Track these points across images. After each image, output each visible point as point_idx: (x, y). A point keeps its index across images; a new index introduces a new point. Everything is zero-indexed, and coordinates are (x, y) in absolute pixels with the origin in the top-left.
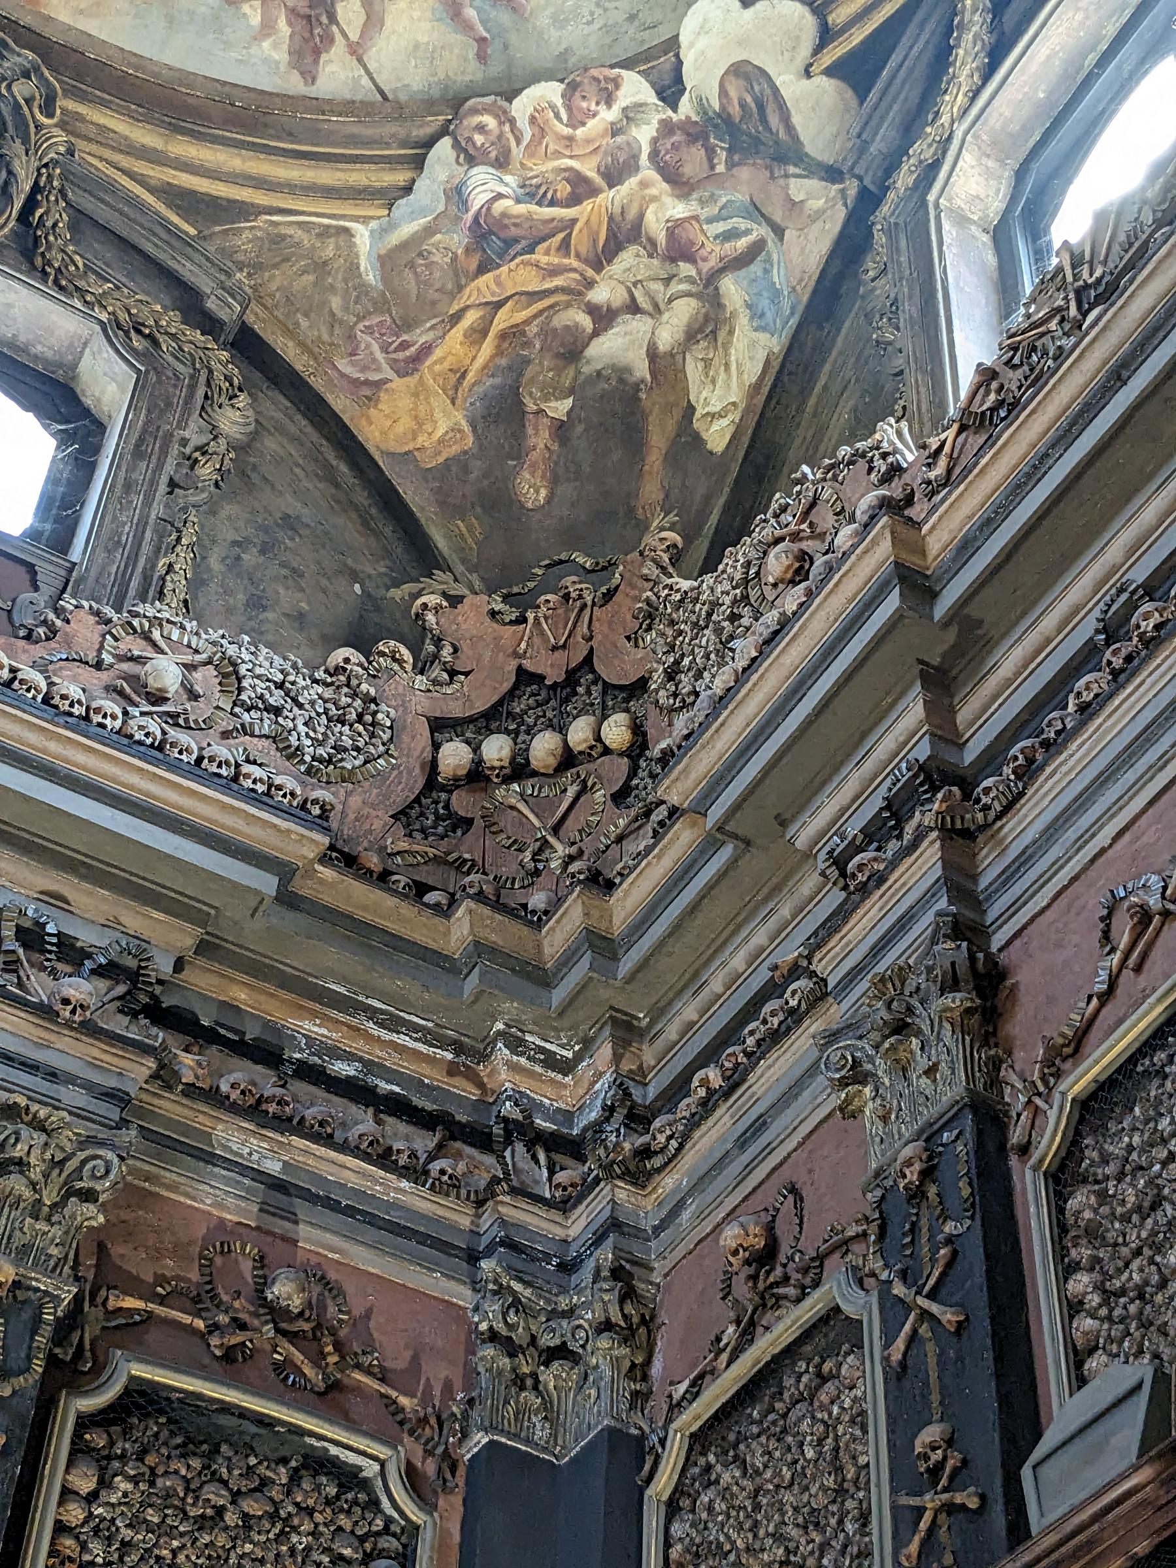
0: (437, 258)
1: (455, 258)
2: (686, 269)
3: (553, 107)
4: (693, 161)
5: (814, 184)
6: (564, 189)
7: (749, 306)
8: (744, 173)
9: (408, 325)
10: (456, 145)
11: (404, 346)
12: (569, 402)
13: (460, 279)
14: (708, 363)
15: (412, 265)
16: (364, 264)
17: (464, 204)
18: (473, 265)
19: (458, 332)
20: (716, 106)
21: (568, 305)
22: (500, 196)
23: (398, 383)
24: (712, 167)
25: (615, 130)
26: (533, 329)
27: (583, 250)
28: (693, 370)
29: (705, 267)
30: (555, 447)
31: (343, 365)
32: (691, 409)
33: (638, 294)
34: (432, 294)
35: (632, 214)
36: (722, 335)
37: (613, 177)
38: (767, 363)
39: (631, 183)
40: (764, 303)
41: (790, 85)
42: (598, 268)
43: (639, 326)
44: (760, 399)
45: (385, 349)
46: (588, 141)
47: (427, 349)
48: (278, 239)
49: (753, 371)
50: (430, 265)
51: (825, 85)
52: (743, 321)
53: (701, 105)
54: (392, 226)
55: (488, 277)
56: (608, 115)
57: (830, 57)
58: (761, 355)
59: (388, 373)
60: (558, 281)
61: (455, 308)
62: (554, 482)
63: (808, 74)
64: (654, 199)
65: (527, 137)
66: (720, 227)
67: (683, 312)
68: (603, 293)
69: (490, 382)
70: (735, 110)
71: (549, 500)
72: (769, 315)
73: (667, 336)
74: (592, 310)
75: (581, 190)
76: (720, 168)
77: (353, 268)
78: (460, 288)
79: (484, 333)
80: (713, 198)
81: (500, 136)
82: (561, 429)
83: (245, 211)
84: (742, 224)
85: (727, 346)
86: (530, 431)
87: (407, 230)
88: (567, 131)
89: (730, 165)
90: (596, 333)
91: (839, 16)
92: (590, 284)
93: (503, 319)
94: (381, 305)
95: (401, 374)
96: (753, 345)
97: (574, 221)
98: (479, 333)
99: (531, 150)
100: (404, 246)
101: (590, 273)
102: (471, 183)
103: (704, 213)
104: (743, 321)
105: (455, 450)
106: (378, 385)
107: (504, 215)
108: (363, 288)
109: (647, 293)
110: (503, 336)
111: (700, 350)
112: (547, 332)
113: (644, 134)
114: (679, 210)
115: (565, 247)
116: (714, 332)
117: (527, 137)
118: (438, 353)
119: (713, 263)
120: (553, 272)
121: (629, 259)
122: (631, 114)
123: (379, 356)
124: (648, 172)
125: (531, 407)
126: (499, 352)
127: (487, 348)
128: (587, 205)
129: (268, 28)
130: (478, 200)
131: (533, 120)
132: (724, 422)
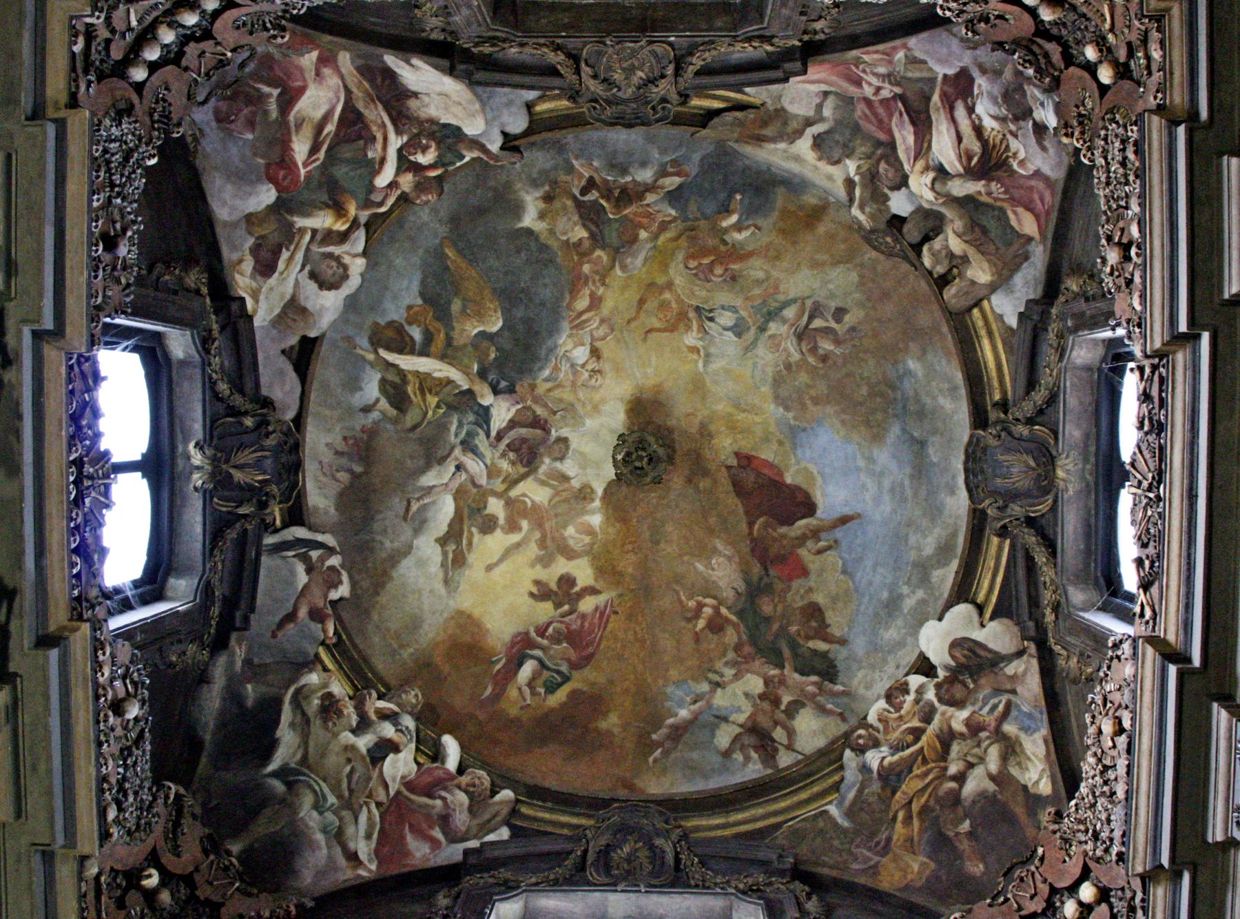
0: (871, 799)
1: (879, 795)
2: (983, 735)
3: (885, 710)
4: (958, 691)
5: (1015, 663)
6: (910, 738)
7: (1021, 729)
8: (983, 681)
9: (873, 834)
10: (853, 750)
11: (878, 843)
12: (967, 822)
13: (886, 800)
14: (1019, 764)
15: (862, 809)
16: (839, 820)
17: (870, 770)
18: (889, 792)
19: (899, 825)
20: (953, 664)
21: (941, 784)
22: (883, 758)
23: (884, 860)
24: (967, 688)
25: (917, 701)
26: (932, 802)
27: (933, 756)
28: (1014, 771)
29: (992, 728)
30: (974, 843)
31: (855, 866)
32: (1025, 787)
33: (970, 759)
34: (878, 815)
35: (945, 728)
36: (1018, 750)
37: (928, 719)
38: (1046, 741)
39: (937, 719)
40: (1027, 722)
41: (979, 635)
42: (946, 761)
43: (979, 771)
44: (1053, 756)
45: (870, 849)
46: (908, 713)
47: (889, 840)
48: (794, 832)
49: (1041, 750)
50: (869, 805)
51: (994, 626)
52: (1023, 736)
53: (947, 668)
54: (843, 798)
55: (899, 794)
56: (910, 698)
57: (988, 615)
58: (1041, 742)
59: (877, 858)
60: (930, 777)
61: (891, 814)
62: (983, 859)
63: (983, 626)
64: (951, 717)
65: (881, 728)
66: (987, 708)
67: (994, 753)
68: (953, 769)
69: (926, 837)
70: (963, 660)
71: (986, 868)
72: (1033, 726)
73: (993, 765)
74: (953, 778)
75: (917, 733)
76: (972, 686)
77: (836, 824)
78: (889, 806)
79: (911, 817)
80: (976, 700)
81: (870, 734)
82: (971, 834)
83: (778, 826)
84: (995, 700)
85: (1023, 751)
86: (957, 844)
87: (851, 795)
88: (897, 715)
89: (975, 681)
90: (961, 787)
91: (980, 598)
92: (946, 769)
93: (915, 807)
94: (857, 832)
95: (882, 856)
96: (1034, 742)
97: (922, 748)
98: (908, 819)
99: (886, 731)
100: (854, 803)
101: (942, 764)
102: (868, 761)
103: (976, 708)
104: (1023, 736)
105: (928, 872)
106: (876, 866)
107: (891, 764)
108: (845, 831)
109: (973, 755)
110: (920, 813)
111: (1012, 761)
112: (937, 801)
113: (931, 695)
114: (965, 714)
115: (925, 761)
116: (1014, 751)
117: (881, 728)
118: (895, 837)
119: (993, 724)
120: (926, 774)
121: (955, 748)
122: (920, 691)
123: (869, 854)
124: (941, 708)
125: (951, 834)
126: (922, 821)
127: (916, 823)
128: (924, 738)
129: (748, 759)
130: (875, 765)
131: (880, 720)
132: (1044, 780)
